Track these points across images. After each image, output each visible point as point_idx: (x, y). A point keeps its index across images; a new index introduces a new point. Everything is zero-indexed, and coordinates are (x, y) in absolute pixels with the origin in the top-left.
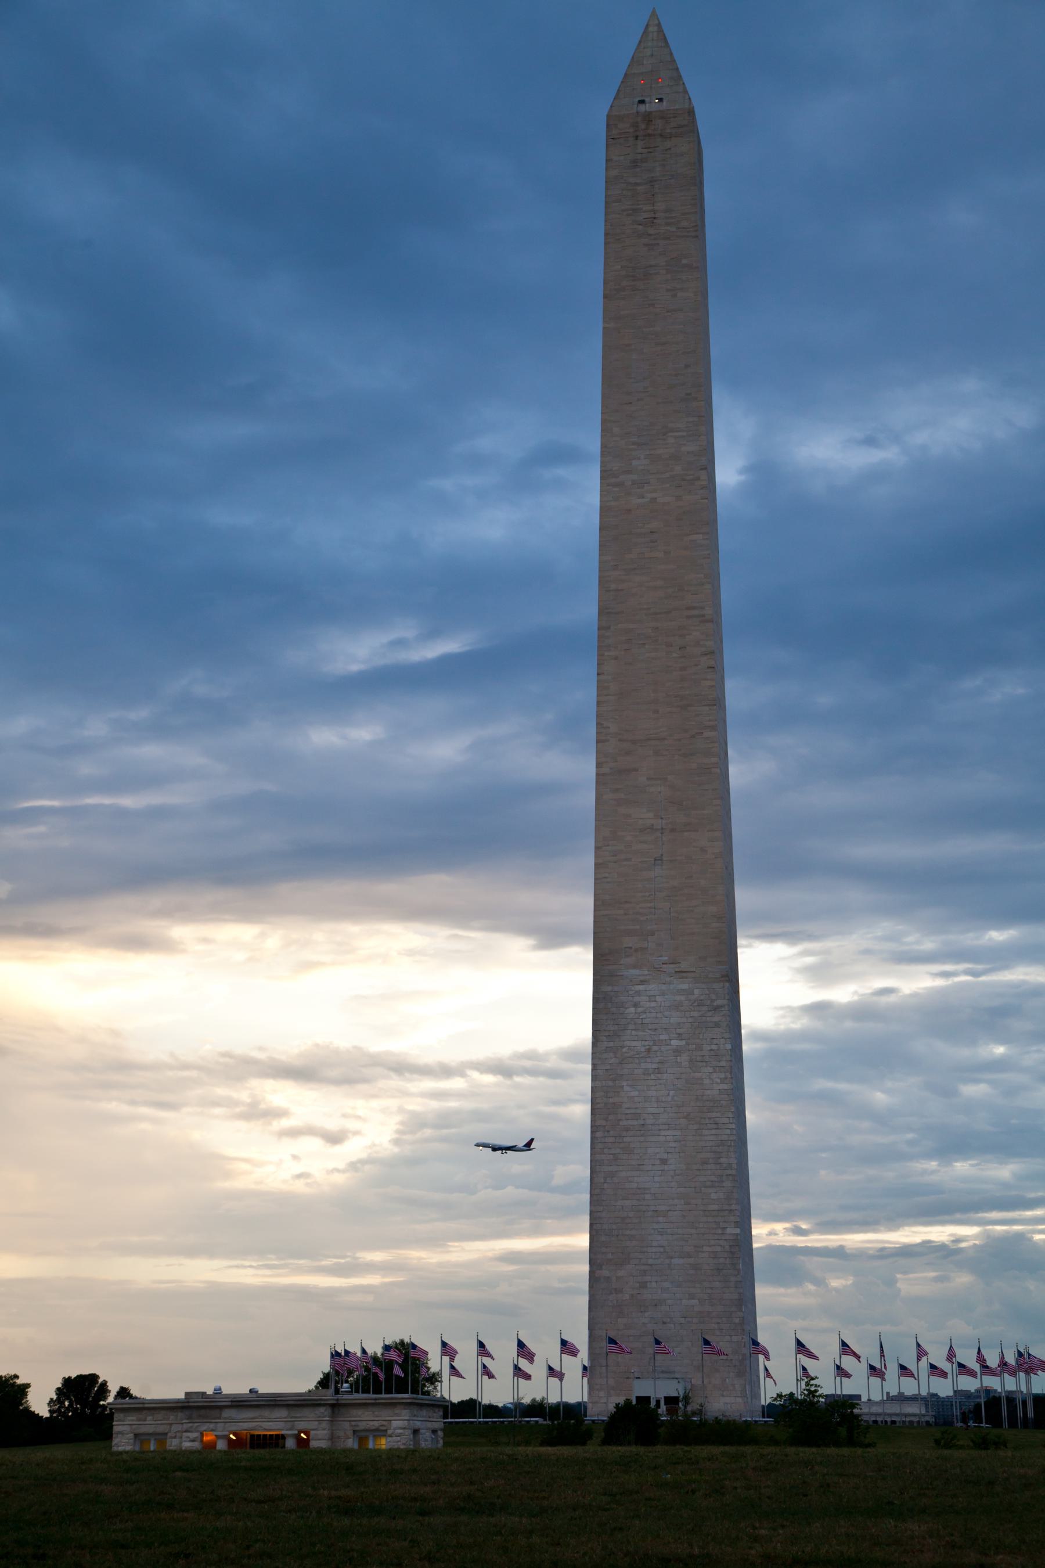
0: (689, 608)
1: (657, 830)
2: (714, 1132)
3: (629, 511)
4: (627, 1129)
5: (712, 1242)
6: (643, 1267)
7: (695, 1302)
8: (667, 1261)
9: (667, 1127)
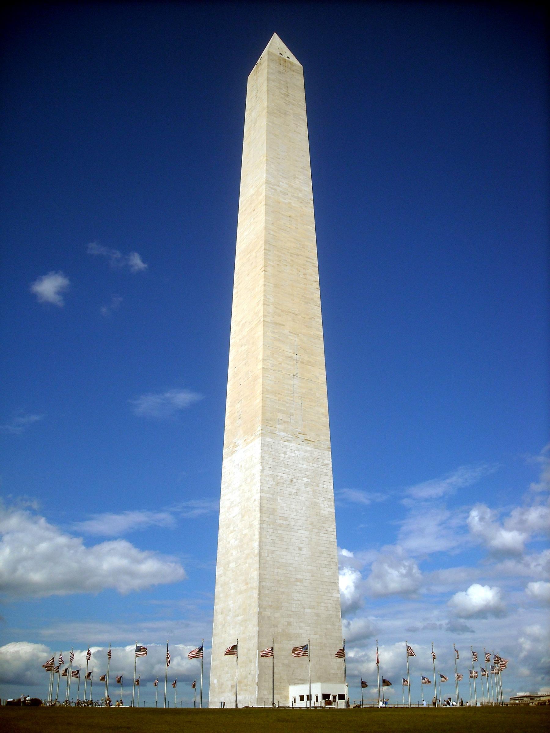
0: (307, 257)
1: (294, 360)
2: (326, 535)
4: (280, 525)
6: (292, 613)
8: (302, 610)
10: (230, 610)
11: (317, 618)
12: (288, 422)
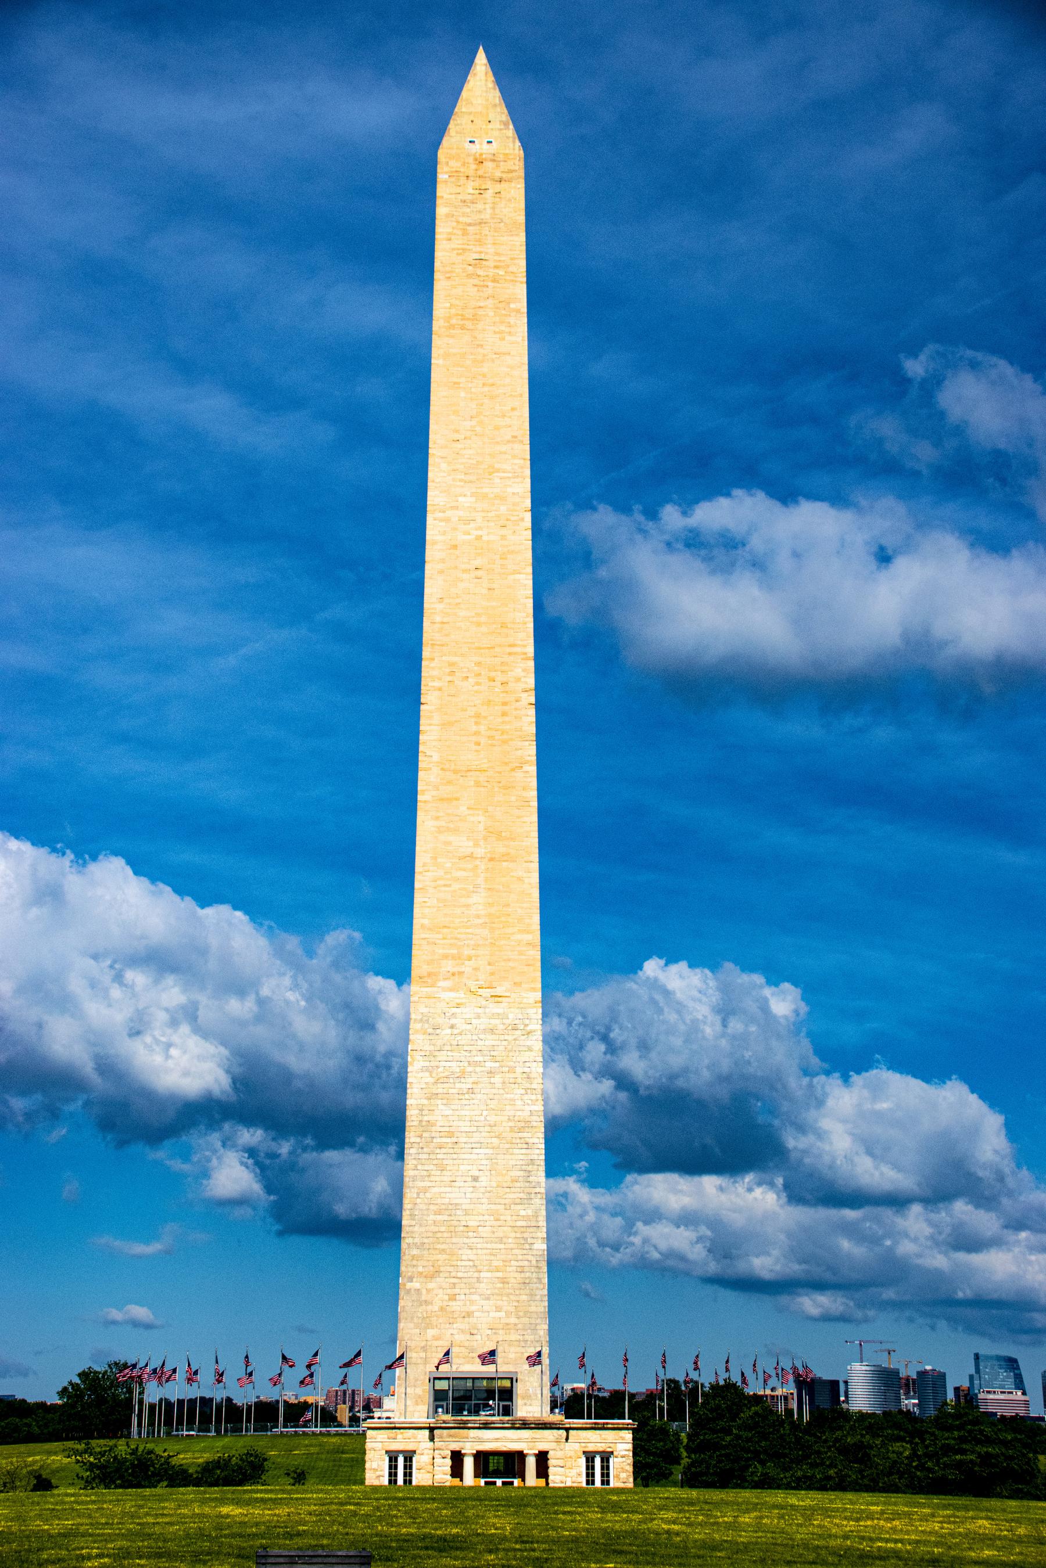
2: (524, 1151)
3: (455, 547)
5: (520, 1257)
7: (503, 1314)
8: (476, 1275)
9: (478, 1145)
11: (501, 1285)
12: (461, 973)
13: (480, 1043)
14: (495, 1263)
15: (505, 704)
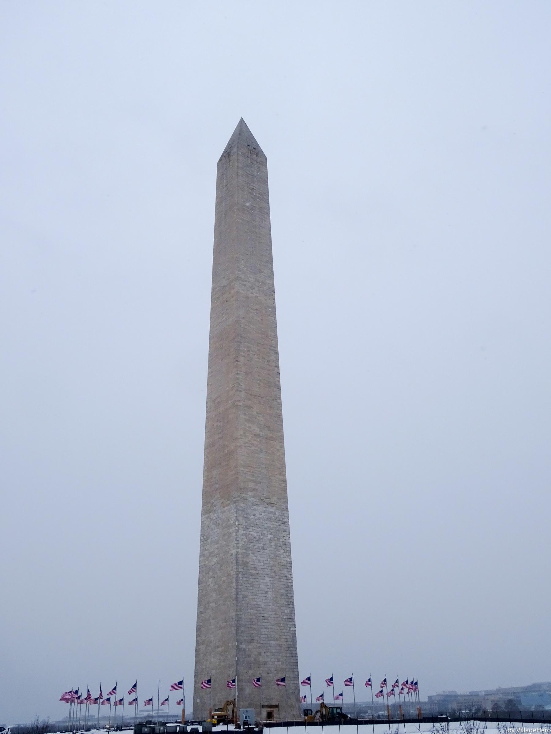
2: (285, 580)
4: (252, 575)
5: (286, 634)
7: (280, 663)
10: (211, 642)
12: (257, 490)
13: (265, 525)
14: (277, 636)
15: (269, 370)
